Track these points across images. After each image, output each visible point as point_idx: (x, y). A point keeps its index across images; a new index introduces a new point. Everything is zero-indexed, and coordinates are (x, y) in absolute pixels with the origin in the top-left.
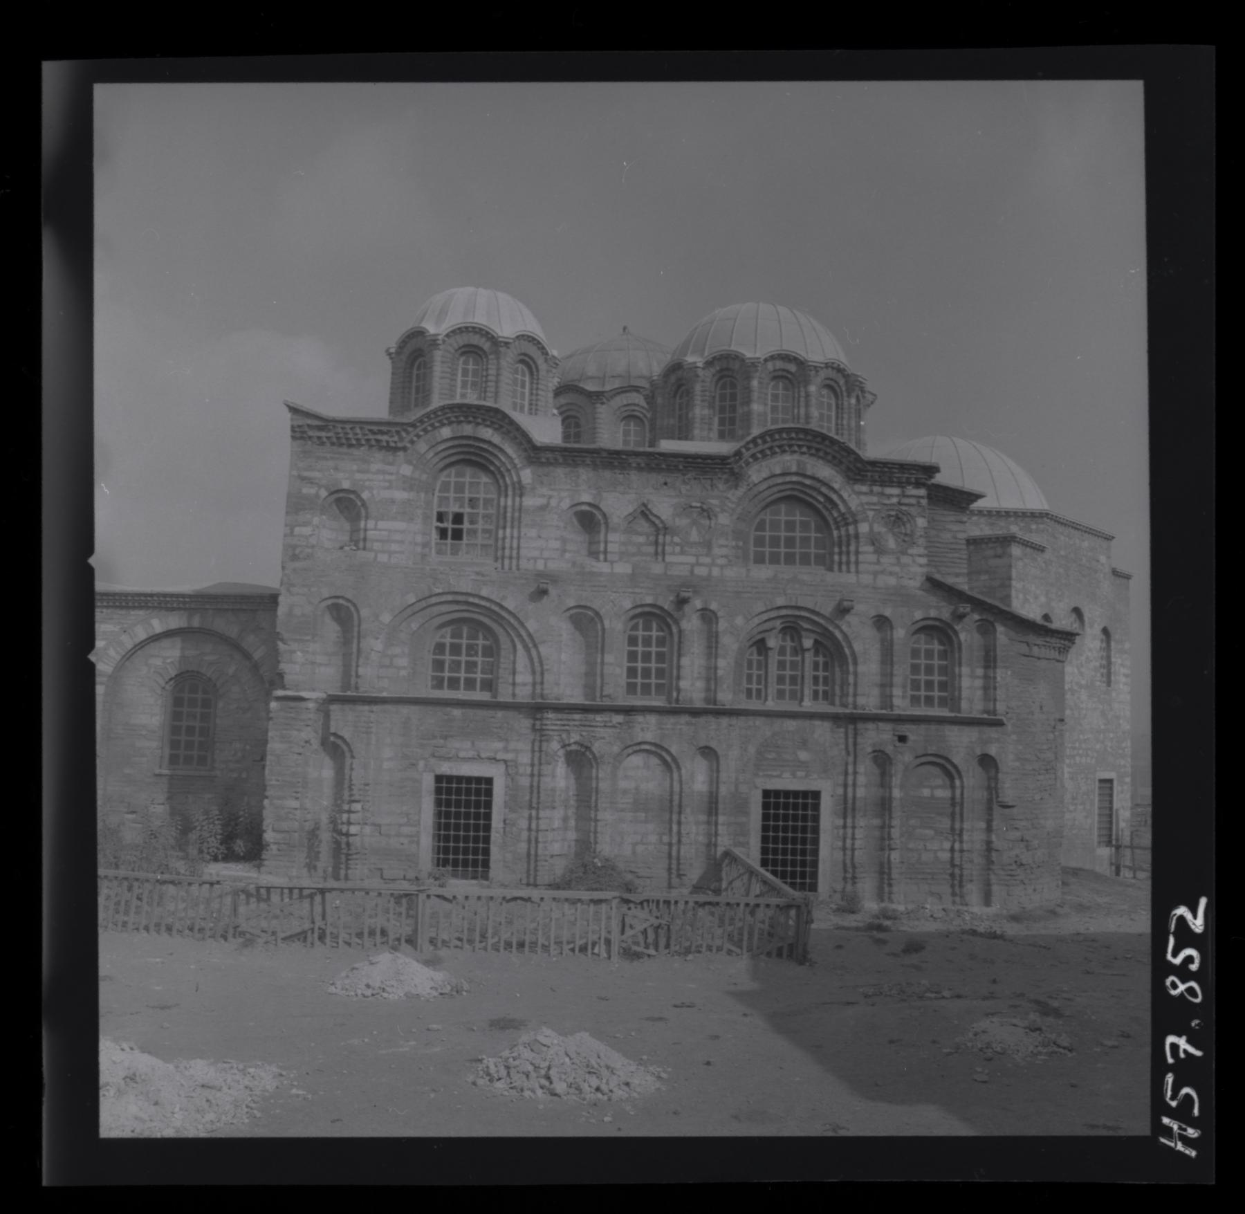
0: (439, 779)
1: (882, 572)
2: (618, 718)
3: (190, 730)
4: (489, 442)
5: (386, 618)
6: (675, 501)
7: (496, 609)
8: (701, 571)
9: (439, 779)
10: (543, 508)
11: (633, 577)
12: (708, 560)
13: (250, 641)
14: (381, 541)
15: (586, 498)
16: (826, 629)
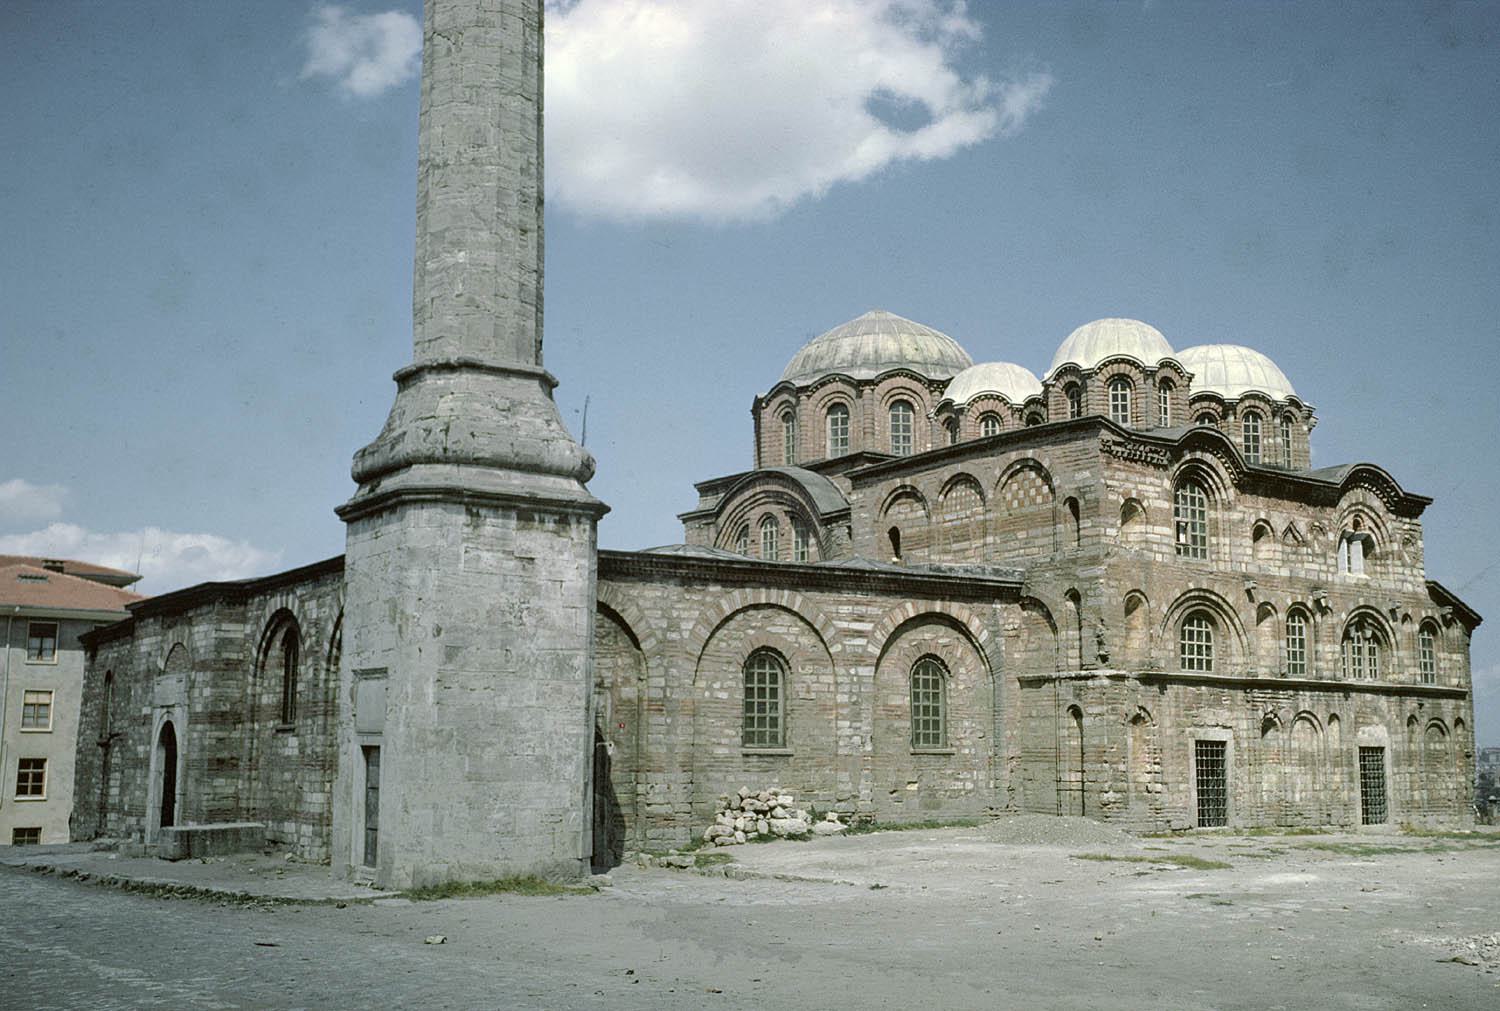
0: (1199, 743)
1: (1406, 581)
2: (1291, 692)
3: (926, 708)
4: (1210, 466)
5: (1165, 609)
6: (1307, 520)
7: (1220, 601)
8: (1323, 576)
9: (1199, 743)
10: (1242, 521)
11: (1291, 580)
12: (1324, 568)
13: (974, 625)
14: (1158, 544)
15: (1263, 516)
16: (1380, 623)
